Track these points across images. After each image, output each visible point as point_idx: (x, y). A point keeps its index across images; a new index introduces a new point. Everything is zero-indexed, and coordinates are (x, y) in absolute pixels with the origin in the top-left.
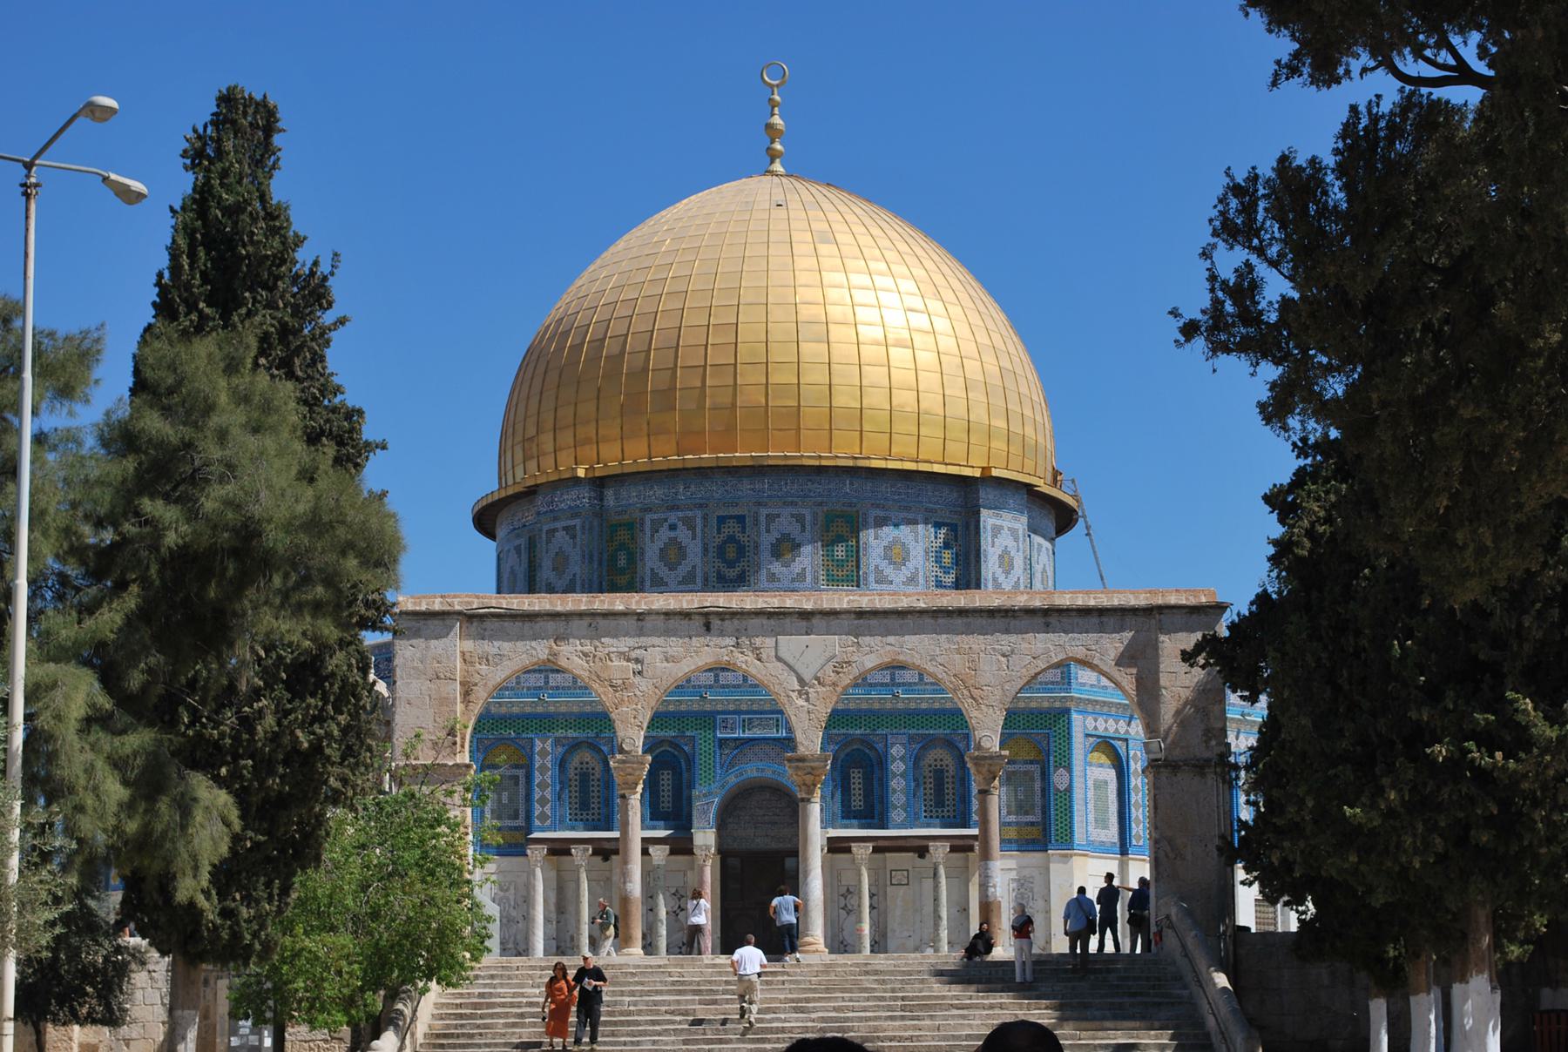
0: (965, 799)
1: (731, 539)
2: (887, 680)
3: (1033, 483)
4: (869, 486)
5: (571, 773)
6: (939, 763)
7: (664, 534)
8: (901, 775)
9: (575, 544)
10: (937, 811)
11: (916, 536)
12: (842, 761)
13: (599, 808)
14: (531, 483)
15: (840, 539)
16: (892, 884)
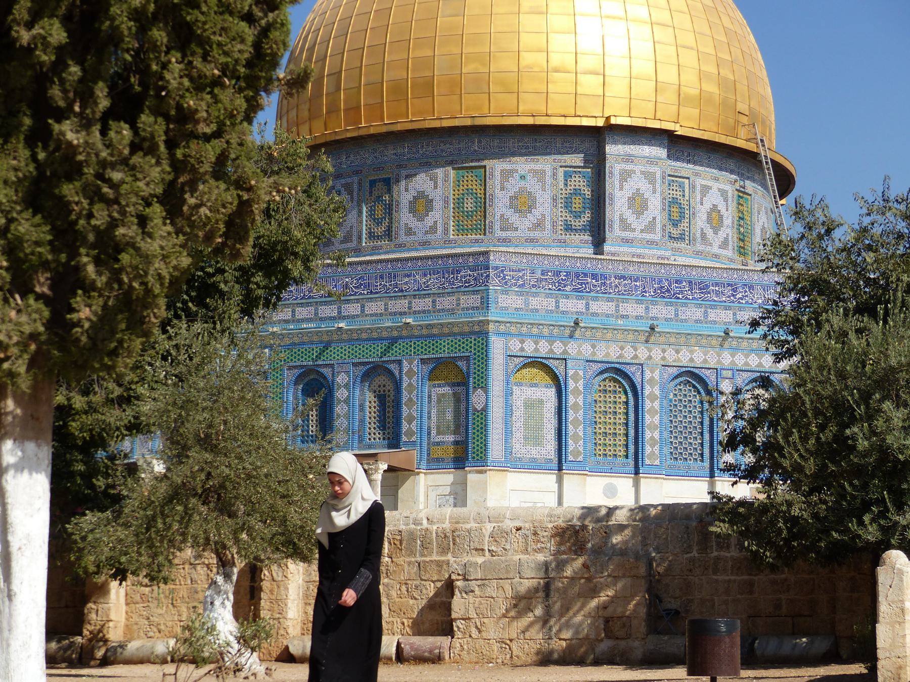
2: (335, 313)
4: (496, 143)
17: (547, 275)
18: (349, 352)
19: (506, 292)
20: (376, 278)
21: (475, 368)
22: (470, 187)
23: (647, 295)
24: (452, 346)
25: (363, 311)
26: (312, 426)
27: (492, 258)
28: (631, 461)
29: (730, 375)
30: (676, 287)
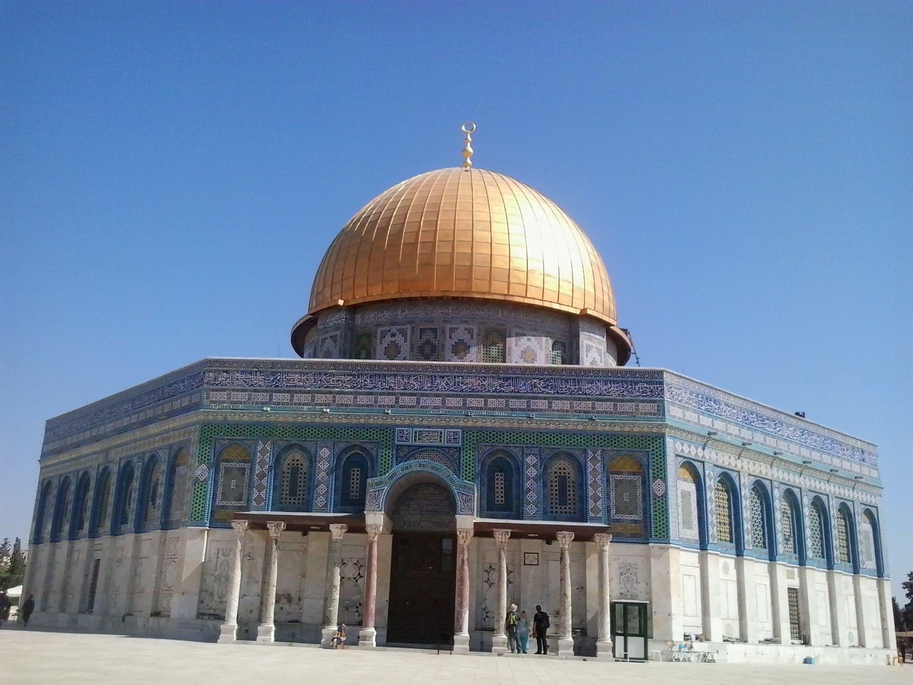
0: (583, 500)
1: (428, 342)
2: (524, 406)
3: (610, 322)
4: (513, 314)
5: (285, 468)
6: (562, 471)
7: (388, 339)
8: (533, 478)
9: (336, 345)
10: (561, 508)
11: (541, 347)
12: (489, 466)
13: (304, 495)
14: (314, 311)
15: (494, 344)
16: (525, 564)
17: (693, 395)
18: (537, 439)
19: (673, 404)
20: (562, 383)
21: (654, 462)
22: (494, 341)
23: (739, 420)
24: (632, 442)
25: (550, 407)
26: (498, 497)
27: (665, 376)
28: (734, 544)
29: (777, 486)
30: (752, 418)
